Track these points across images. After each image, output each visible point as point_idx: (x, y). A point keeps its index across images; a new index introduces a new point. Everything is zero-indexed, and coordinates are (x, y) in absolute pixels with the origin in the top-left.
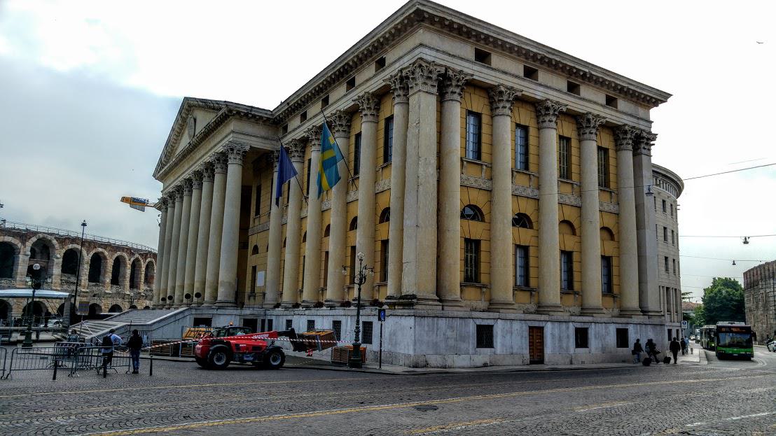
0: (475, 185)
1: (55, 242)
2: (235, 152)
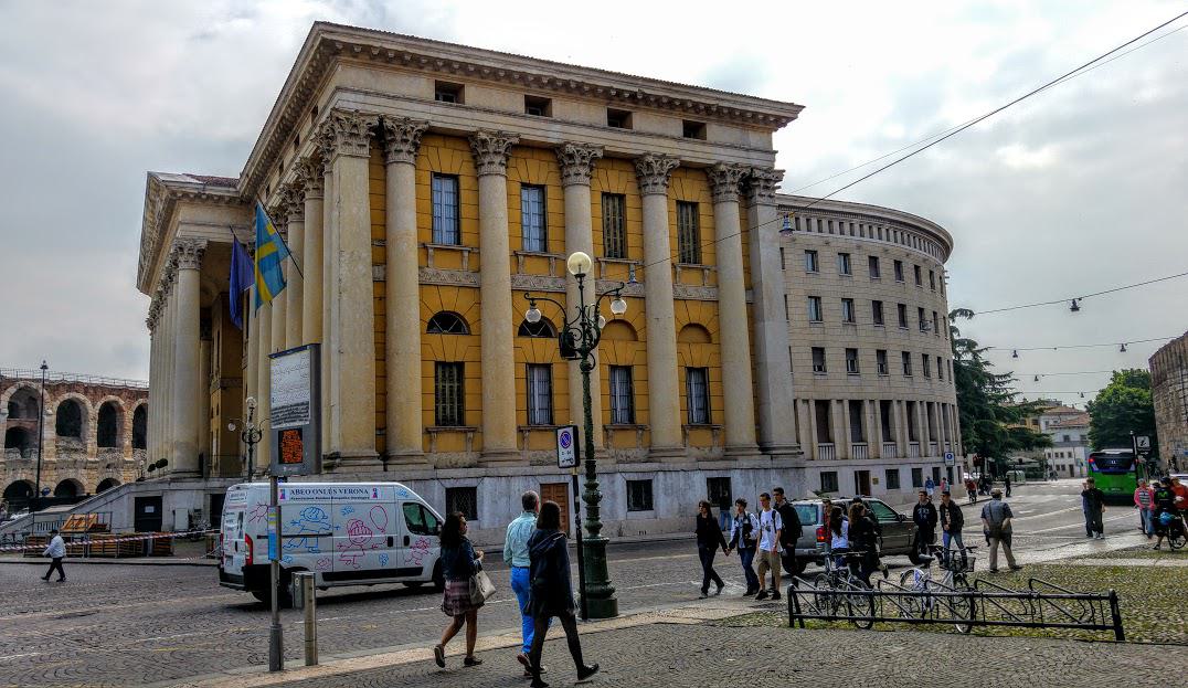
0: (449, 281)
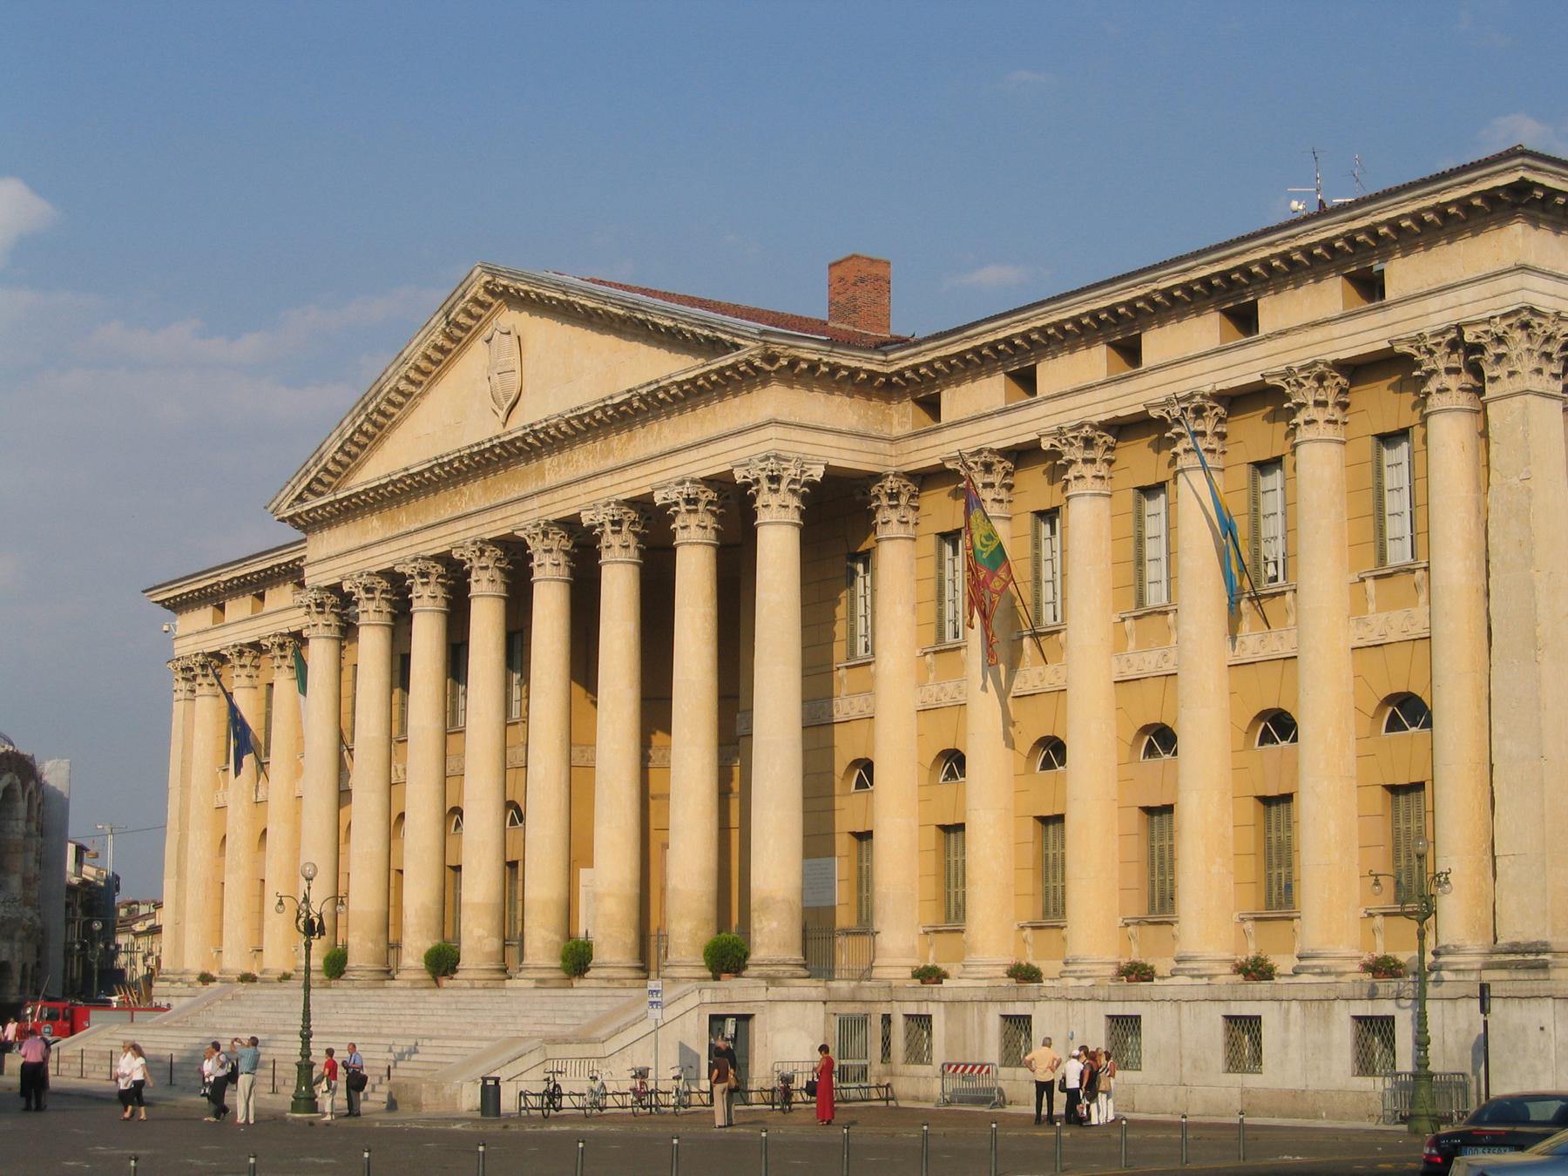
2: (783, 486)
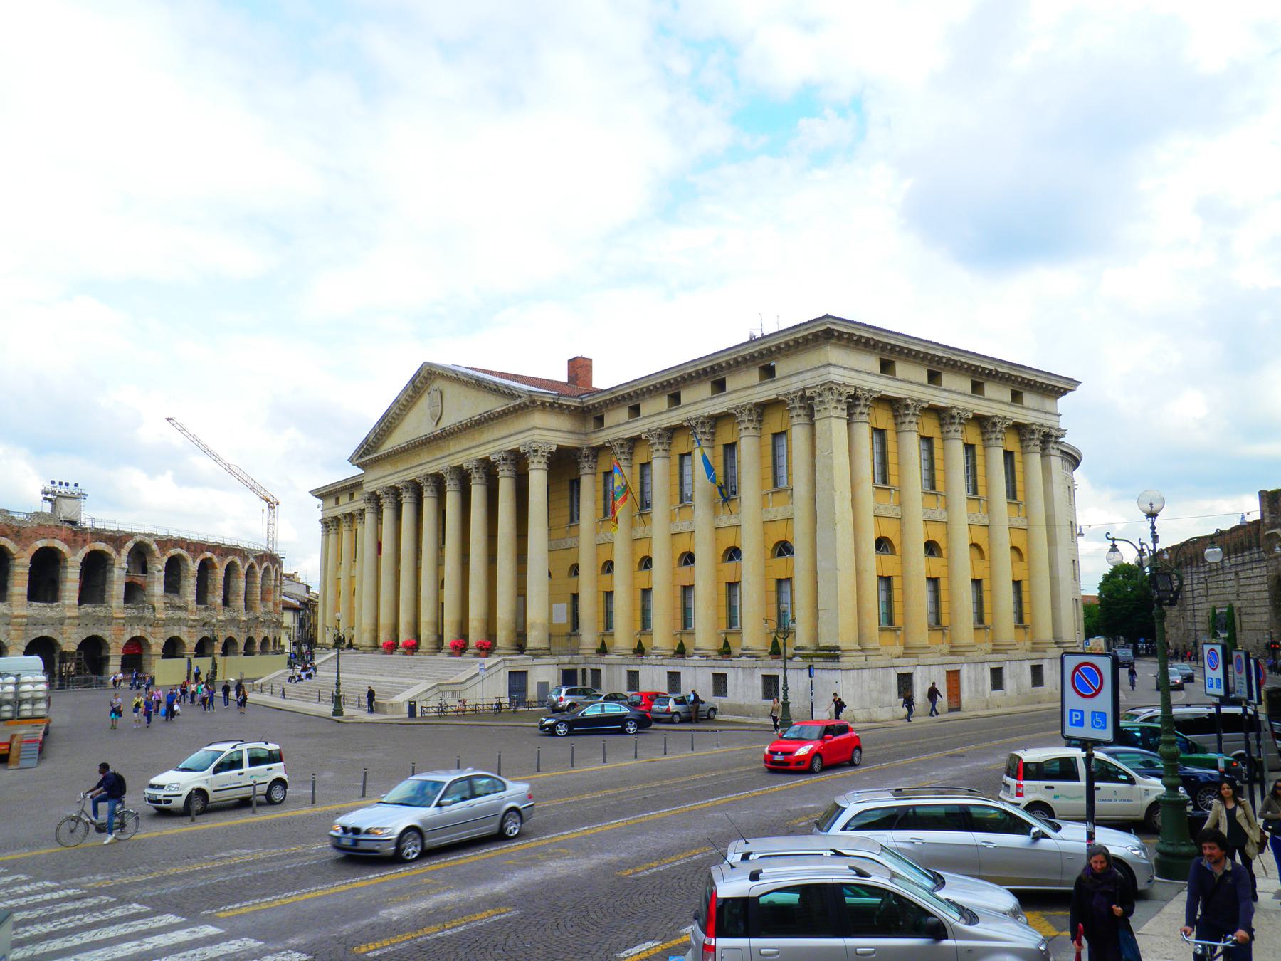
1: (154, 547)
